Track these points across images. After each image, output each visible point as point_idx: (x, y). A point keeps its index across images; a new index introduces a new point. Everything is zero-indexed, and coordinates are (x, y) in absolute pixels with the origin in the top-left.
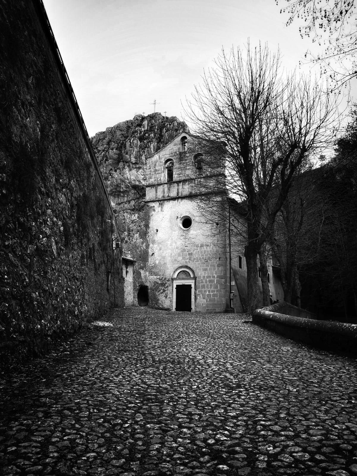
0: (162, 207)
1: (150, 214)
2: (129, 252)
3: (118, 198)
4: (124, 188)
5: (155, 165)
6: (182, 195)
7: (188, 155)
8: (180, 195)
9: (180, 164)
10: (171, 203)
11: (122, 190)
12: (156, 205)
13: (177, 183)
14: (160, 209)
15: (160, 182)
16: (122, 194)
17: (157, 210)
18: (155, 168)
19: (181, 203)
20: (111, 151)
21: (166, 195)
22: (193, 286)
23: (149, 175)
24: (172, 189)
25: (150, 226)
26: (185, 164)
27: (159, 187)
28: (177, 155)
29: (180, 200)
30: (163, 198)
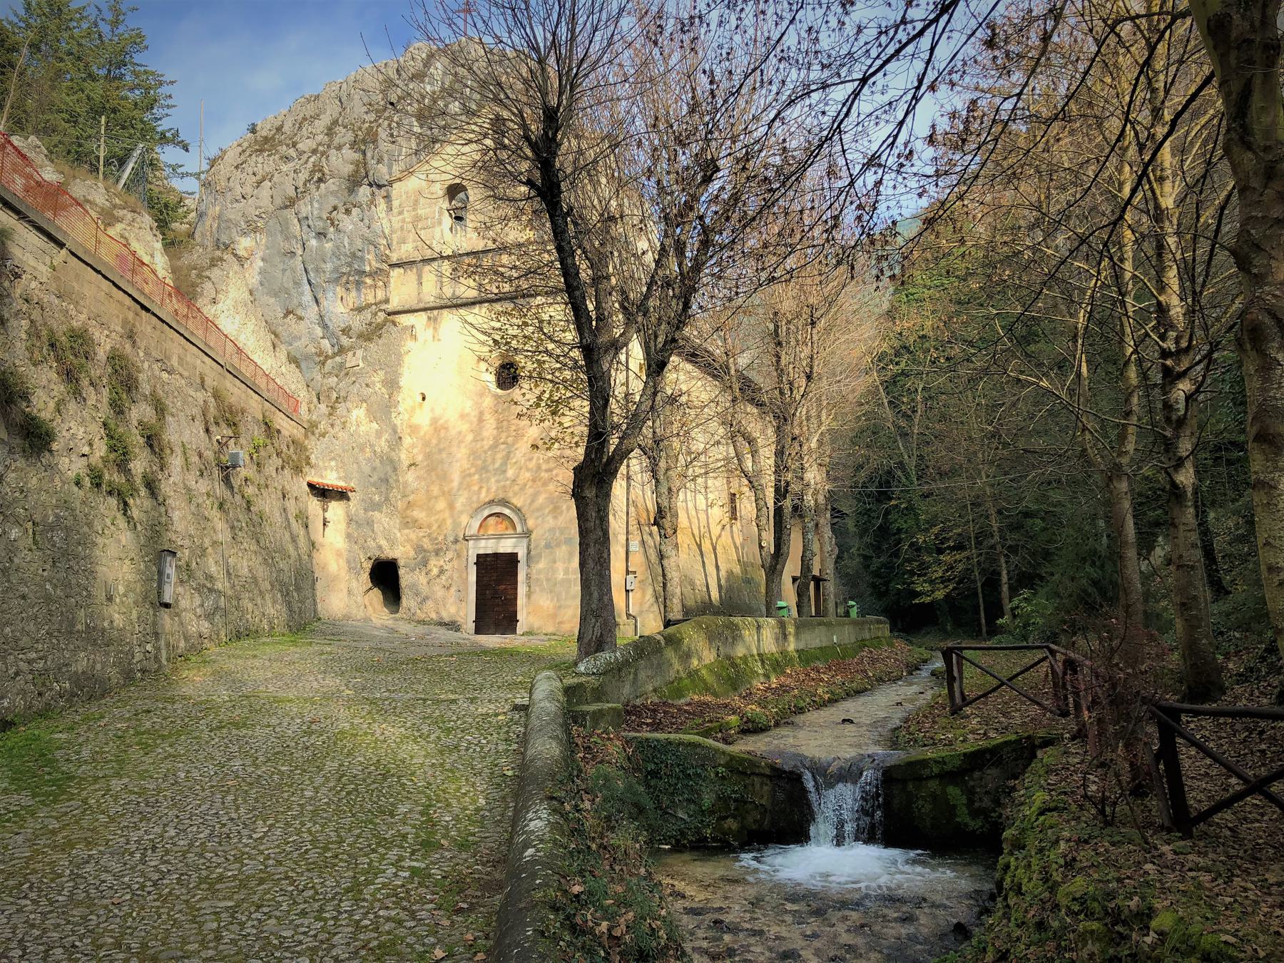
0: (435, 329)
2: (333, 463)
3: (358, 290)
4: (374, 263)
5: (416, 202)
11: (368, 269)
12: (419, 320)
14: (430, 331)
16: (369, 281)
18: (414, 209)
20: (333, 152)
21: (448, 291)
22: (522, 556)
25: (401, 384)
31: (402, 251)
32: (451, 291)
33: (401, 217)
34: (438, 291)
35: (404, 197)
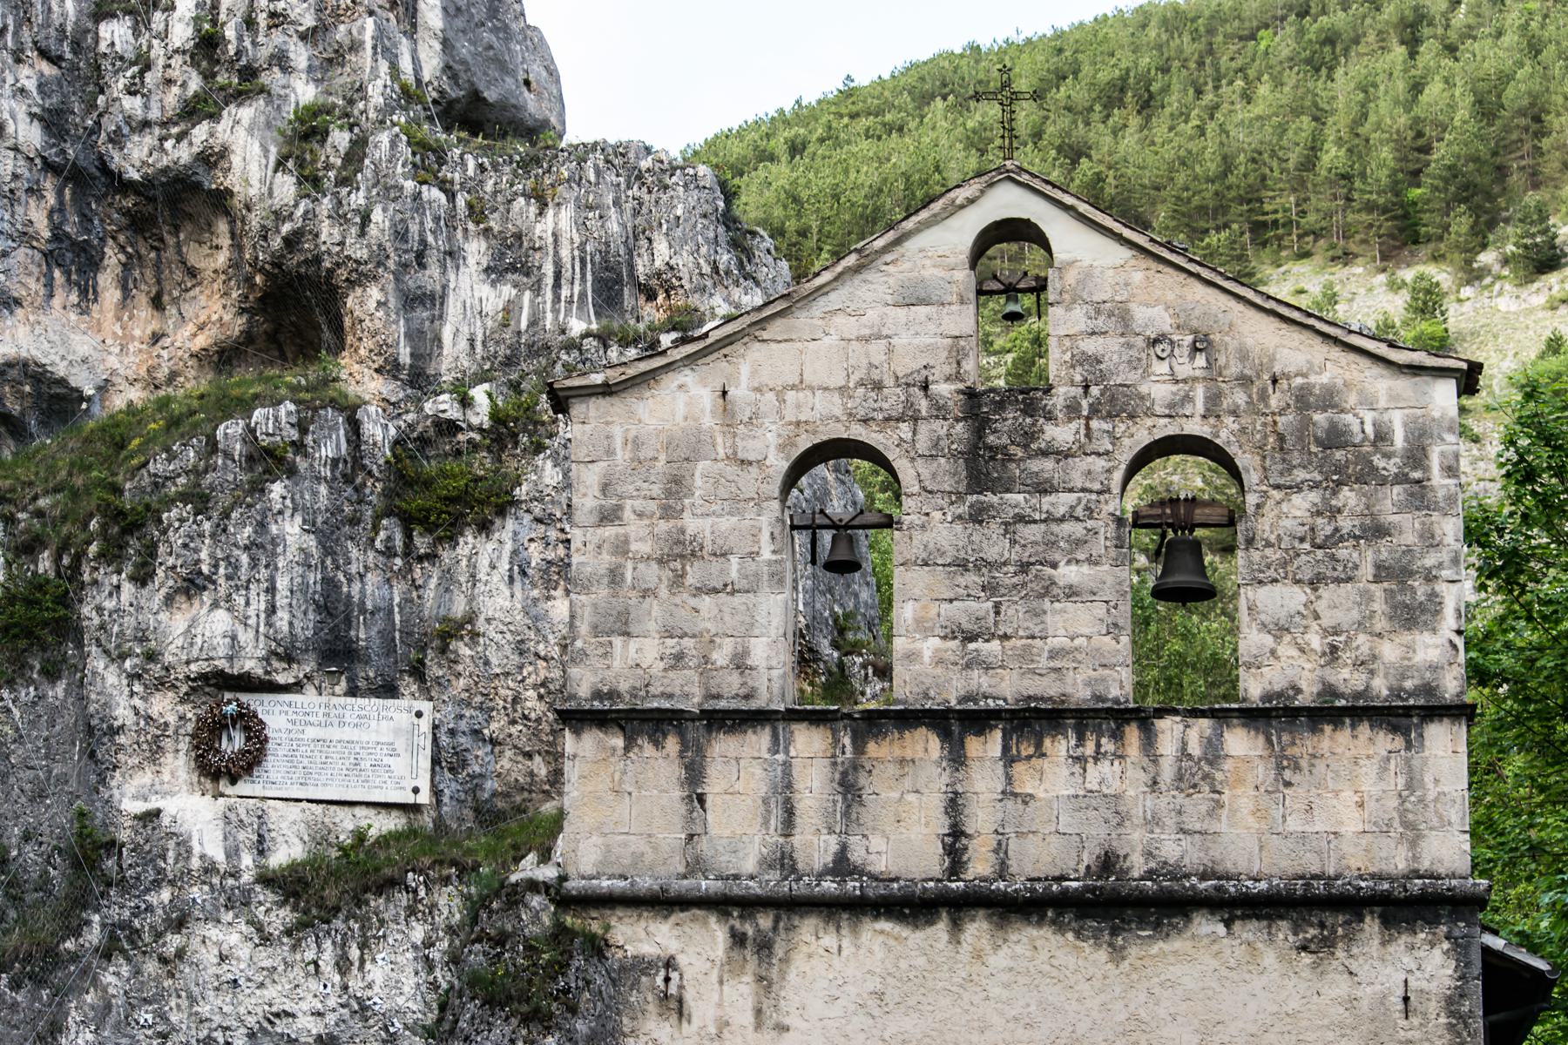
0: (764, 982)
5: (676, 486)
6: (1002, 872)
7: (1061, 433)
8: (979, 866)
9: (978, 516)
10: (878, 935)
13: (945, 735)
14: (741, 994)
15: (731, 683)
17: (702, 1008)
18: (668, 512)
19: (999, 960)
23: (602, 592)
24: (881, 787)
27: (723, 747)
28: (939, 411)
29: (977, 929)
30: (771, 883)
31: (617, 664)
32: (833, 844)
33: (609, 532)
35: (622, 456)
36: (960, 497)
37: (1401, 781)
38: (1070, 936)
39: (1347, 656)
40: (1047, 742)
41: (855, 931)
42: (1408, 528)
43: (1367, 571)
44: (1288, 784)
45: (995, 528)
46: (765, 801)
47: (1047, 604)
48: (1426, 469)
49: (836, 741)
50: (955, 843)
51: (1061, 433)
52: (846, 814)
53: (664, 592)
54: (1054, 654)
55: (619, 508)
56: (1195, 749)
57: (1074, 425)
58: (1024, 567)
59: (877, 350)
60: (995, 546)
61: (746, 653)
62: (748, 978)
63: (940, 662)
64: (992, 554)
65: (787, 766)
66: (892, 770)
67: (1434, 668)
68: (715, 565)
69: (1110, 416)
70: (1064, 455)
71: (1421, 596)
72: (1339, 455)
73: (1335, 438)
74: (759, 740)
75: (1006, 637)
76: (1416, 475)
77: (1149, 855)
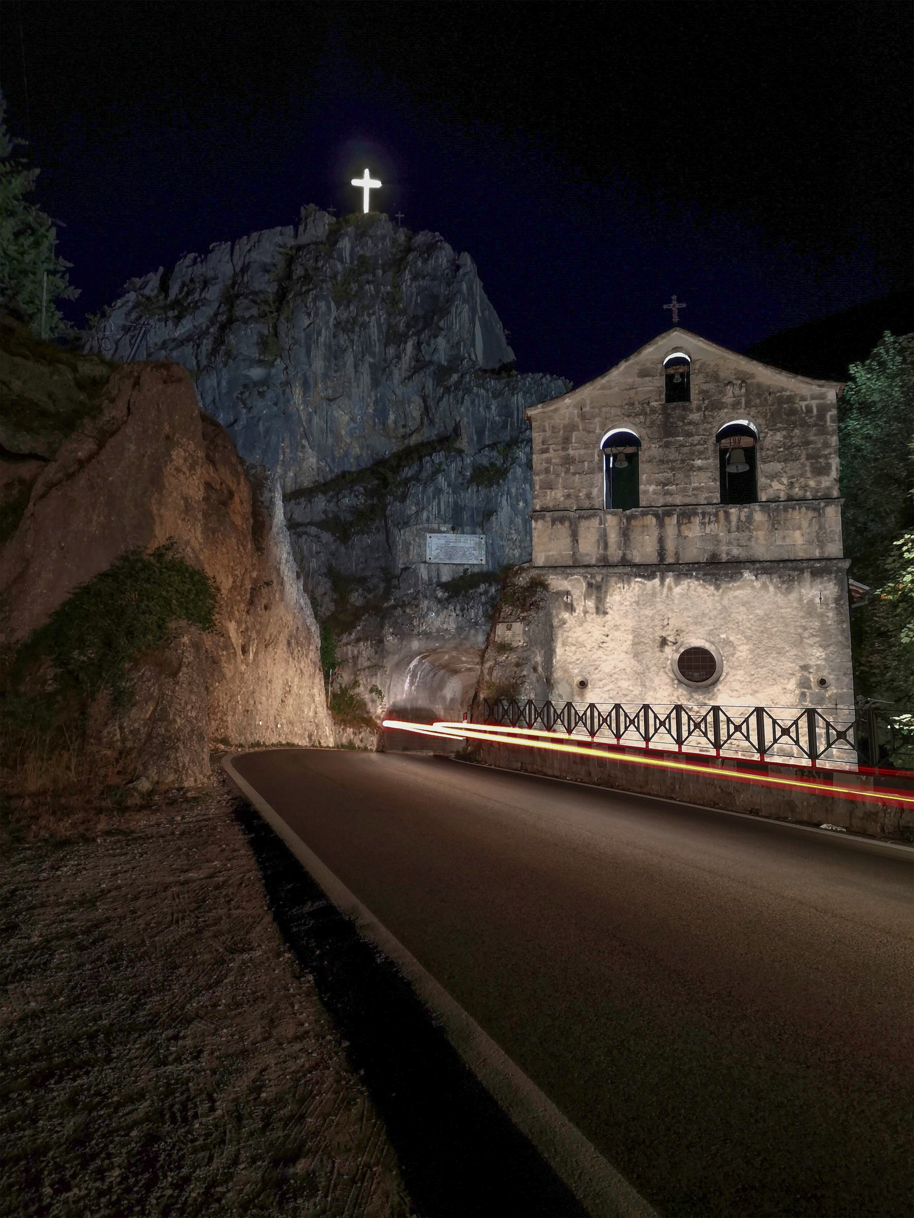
1: (555, 622)
5: (566, 441)
7: (695, 416)
8: (670, 560)
9: (667, 445)
14: (591, 604)
17: (579, 610)
19: (677, 590)
21: (615, 553)
24: (636, 536)
26: (685, 450)
27: (584, 524)
33: (545, 456)
34: (601, 552)
36: (661, 440)
37: (817, 527)
38: (701, 582)
39: (797, 485)
40: (692, 518)
41: (629, 583)
42: (819, 441)
43: (803, 457)
44: (776, 529)
45: (673, 450)
46: (598, 541)
47: (691, 473)
48: (825, 422)
49: (621, 520)
50: (662, 553)
51: (695, 416)
52: (625, 544)
53: (563, 474)
54: (694, 489)
55: (548, 449)
56: (743, 518)
57: (699, 414)
58: (683, 461)
59: (632, 392)
60: (673, 455)
61: (591, 493)
62: (594, 597)
63: (655, 493)
64: (672, 457)
65: (605, 529)
66: (640, 529)
67: (828, 488)
68: (580, 465)
69: (711, 411)
70: (696, 424)
71: (823, 464)
72: (793, 418)
73: (793, 412)
74: (595, 522)
75: (677, 484)
76: (822, 423)
77: (728, 554)
